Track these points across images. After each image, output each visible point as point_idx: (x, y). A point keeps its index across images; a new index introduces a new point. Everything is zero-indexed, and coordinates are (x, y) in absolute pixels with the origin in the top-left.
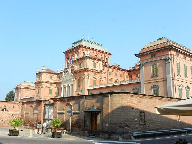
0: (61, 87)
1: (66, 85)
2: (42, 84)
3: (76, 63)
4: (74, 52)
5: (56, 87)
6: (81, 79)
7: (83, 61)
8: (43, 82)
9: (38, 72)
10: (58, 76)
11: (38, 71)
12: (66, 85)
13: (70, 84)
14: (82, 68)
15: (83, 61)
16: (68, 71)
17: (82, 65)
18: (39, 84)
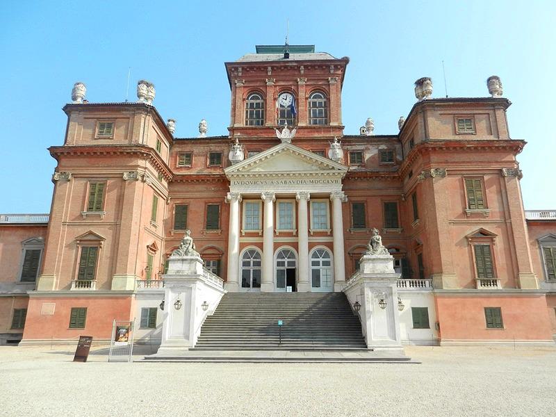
0: (229, 197)
1: (268, 191)
2: (141, 162)
3: (439, 112)
4: (300, 76)
5: (166, 193)
6: (486, 178)
7: (487, 112)
8: (137, 155)
9: (79, 101)
10: (177, 149)
11: (86, 95)
12: (268, 191)
13: (302, 191)
14: (483, 135)
15: (487, 112)
16: (278, 141)
17: (482, 124)
18: (120, 161)
